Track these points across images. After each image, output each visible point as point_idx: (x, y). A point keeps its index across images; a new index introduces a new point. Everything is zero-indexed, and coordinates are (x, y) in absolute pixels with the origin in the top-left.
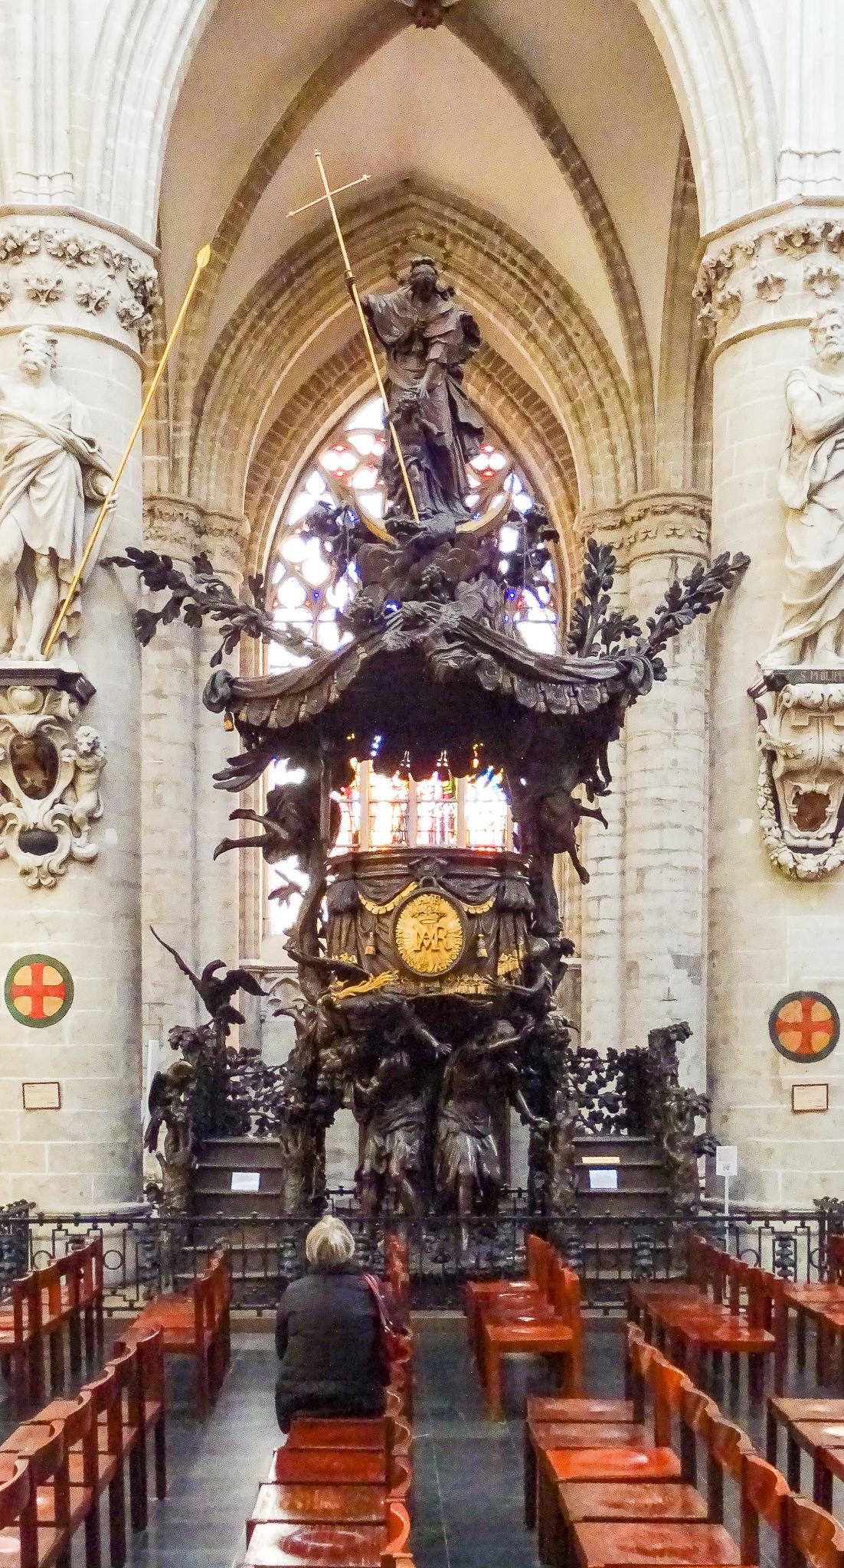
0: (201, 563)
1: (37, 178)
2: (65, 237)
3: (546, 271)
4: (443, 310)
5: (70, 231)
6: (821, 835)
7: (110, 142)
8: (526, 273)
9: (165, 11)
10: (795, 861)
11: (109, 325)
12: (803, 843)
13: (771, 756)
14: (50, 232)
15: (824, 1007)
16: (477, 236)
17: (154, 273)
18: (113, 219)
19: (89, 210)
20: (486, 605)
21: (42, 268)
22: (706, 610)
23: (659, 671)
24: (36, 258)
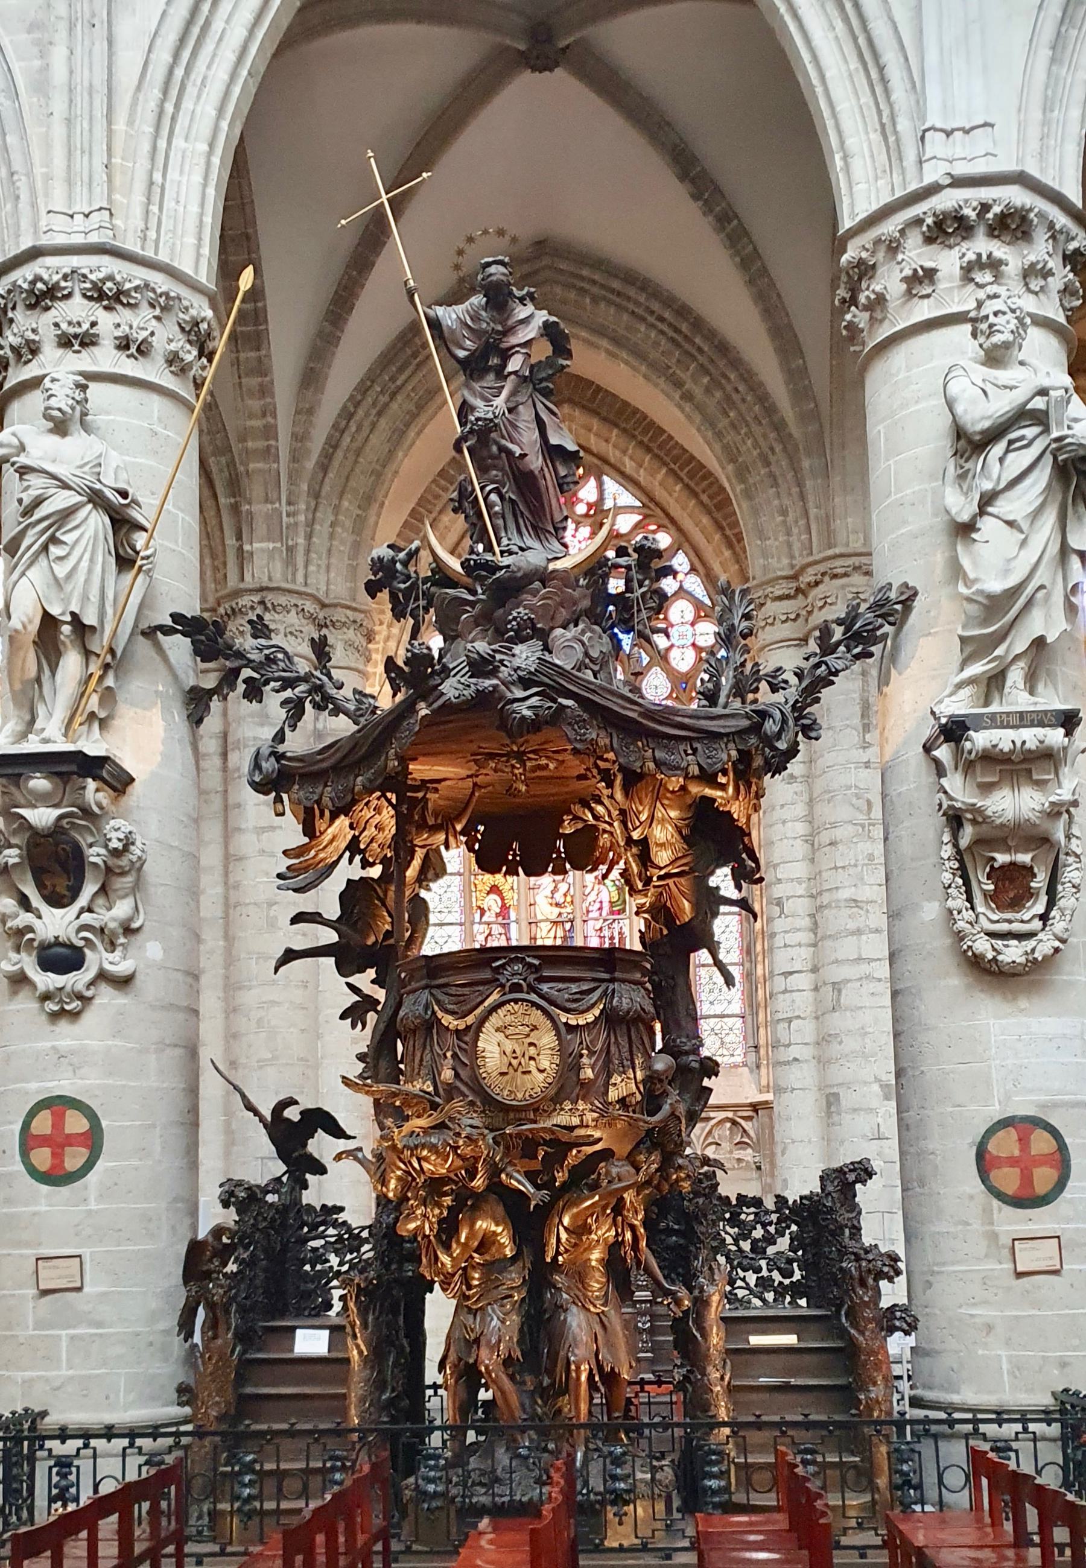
1: (72, 216)
2: (101, 275)
3: (698, 324)
4: (522, 316)
6: (1026, 917)
8: (677, 330)
9: (220, 39)
10: (994, 949)
12: (1004, 927)
13: (955, 820)
14: (85, 271)
15: (1047, 1135)
16: (619, 294)
18: (163, 257)
19: (132, 245)
20: (586, 654)
24: (69, 302)
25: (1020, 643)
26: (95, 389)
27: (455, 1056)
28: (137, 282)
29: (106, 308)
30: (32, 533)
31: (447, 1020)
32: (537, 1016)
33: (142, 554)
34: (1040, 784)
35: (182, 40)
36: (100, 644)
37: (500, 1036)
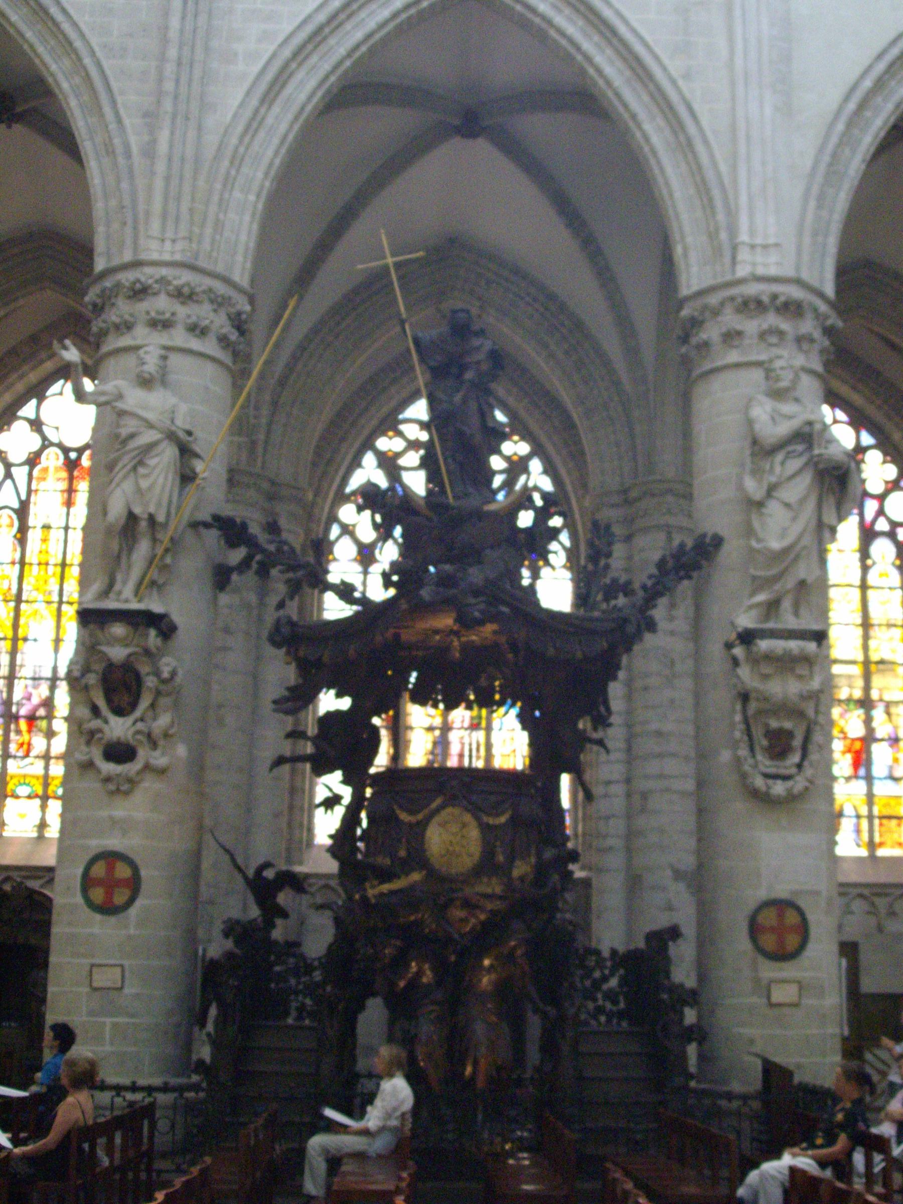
0: (273, 528)
3: (563, 307)
5: (185, 277)
7: (221, 216)
11: (210, 346)
13: (745, 697)
14: (170, 278)
16: (507, 280)
17: (248, 308)
18: (220, 268)
19: (202, 263)
21: (162, 303)
22: (690, 578)
23: (651, 626)
25: (790, 583)
26: (175, 360)
27: (408, 842)
28: (203, 288)
29: (183, 303)
30: (126, 459)
31: (404, 816)
32: (468, 818)
33: (201, 476)
34: (800, 677)
35: (246, 131)
36: (165, 537)
37: (442, 830)
